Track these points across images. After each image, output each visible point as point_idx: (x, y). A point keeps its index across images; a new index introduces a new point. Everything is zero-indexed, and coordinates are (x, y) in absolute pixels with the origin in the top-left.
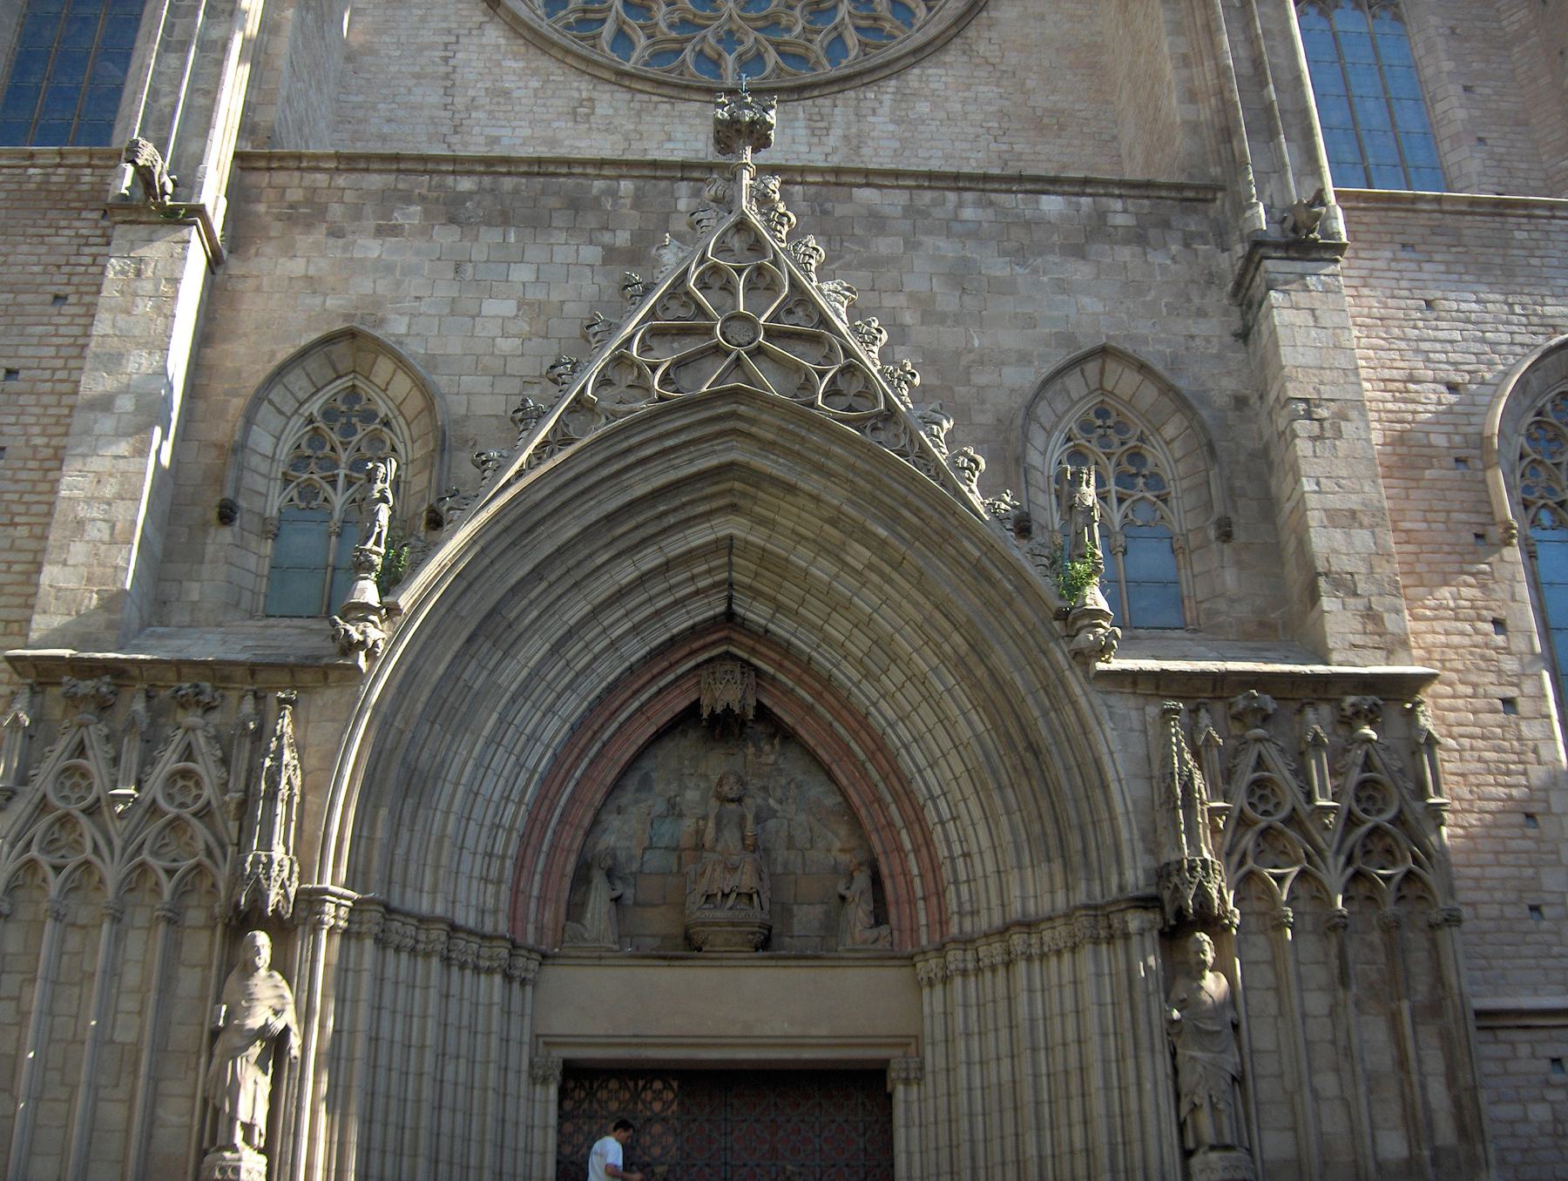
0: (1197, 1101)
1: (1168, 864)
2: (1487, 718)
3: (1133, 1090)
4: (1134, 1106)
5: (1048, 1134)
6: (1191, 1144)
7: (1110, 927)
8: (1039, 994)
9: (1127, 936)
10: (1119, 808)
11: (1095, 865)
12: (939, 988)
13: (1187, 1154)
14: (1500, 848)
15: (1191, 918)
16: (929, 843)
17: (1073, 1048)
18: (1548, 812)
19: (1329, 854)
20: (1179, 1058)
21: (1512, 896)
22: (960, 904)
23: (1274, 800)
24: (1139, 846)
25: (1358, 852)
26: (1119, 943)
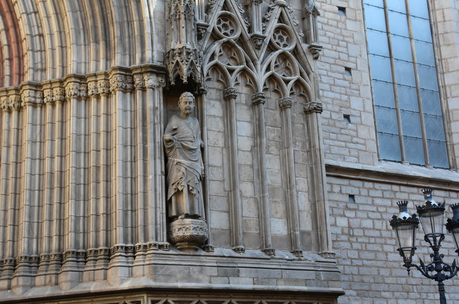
0: (180, 189)
1: (173, 50)
2: (330, 15)
3: (140, 180)
4: (140, 188)
5: (82, 203)
6: (174, 214)
7: (133, 83)
8: (83, 120)
9: (143, 89)
10: (146, 14)
11: (127, 46)
12: (14, 114)
13: (170, 220)
14: (332, 82)
15: (185, 81)
16: (16, 26)
17: (102, 153)
18: (356, 69)
19: (259, 62)
20: (170, 163)
21: (337, 109)
22: (34, 64)
23: (231, 28)
24: (155, 38)
25: (273, 65)
26: (139, 93)
